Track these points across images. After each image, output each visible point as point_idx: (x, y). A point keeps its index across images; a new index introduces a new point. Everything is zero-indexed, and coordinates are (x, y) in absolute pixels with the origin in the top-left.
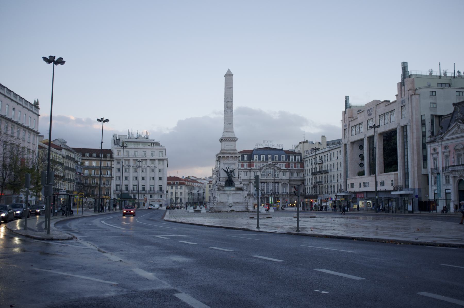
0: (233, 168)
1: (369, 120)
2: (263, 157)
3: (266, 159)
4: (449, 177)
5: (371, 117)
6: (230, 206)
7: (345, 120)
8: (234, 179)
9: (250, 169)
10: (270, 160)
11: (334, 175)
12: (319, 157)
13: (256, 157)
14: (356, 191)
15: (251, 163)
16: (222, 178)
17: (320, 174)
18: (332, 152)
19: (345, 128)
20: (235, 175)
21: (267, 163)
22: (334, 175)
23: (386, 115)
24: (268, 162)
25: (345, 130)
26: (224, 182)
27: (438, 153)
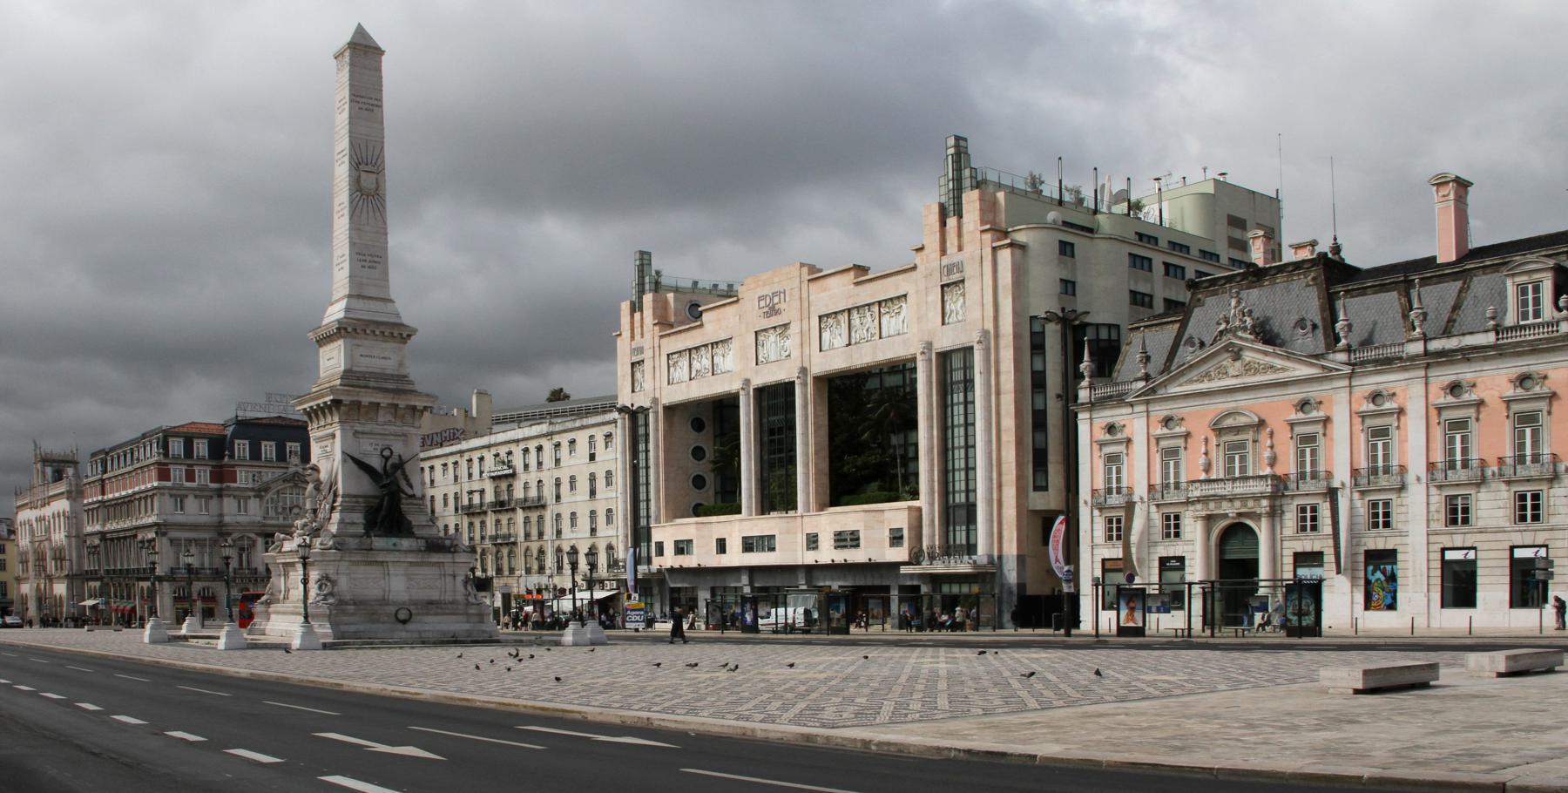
1: (765, 330)
2: (268, 448)
3: (282, 456)
4: (1177, 518)
5: (775, 321)
7: (637, 331)
9: (221, 490)
10: (295, 460)
11: (573, 514)
12: (497, 455)
13: (242, 447)
14: (685, 566)
15: (221, 466)
17: (500, 511)
18: (556, 438)
19: (635, 359)
21: (284, 471)
22: (573, 514)
23: (855, 315)
24: (287, 468)
25: (633, 365)
27: (1129, 441)
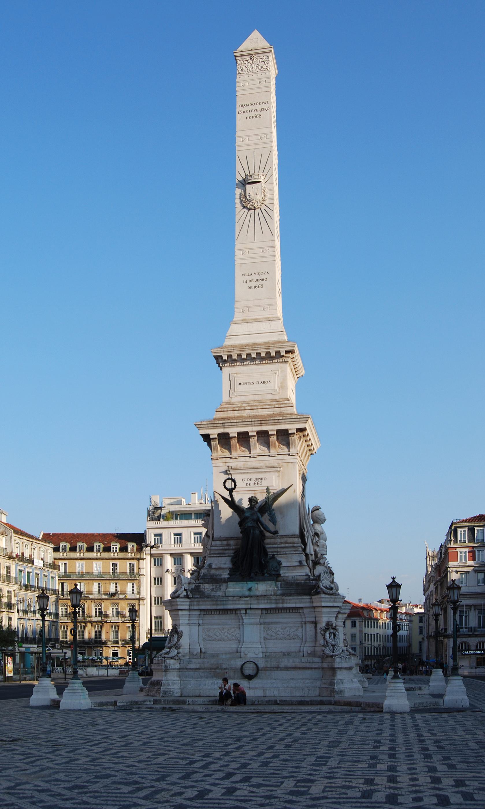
0: (268, 489)
6: (248, 672)
8: (278, 540)
16: (221, 539)
20: (274, 521)
26: (228, 559)
